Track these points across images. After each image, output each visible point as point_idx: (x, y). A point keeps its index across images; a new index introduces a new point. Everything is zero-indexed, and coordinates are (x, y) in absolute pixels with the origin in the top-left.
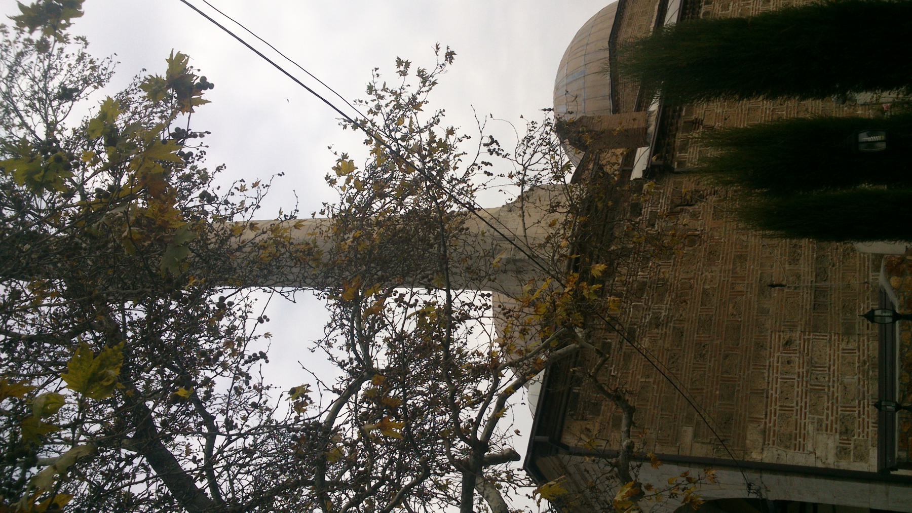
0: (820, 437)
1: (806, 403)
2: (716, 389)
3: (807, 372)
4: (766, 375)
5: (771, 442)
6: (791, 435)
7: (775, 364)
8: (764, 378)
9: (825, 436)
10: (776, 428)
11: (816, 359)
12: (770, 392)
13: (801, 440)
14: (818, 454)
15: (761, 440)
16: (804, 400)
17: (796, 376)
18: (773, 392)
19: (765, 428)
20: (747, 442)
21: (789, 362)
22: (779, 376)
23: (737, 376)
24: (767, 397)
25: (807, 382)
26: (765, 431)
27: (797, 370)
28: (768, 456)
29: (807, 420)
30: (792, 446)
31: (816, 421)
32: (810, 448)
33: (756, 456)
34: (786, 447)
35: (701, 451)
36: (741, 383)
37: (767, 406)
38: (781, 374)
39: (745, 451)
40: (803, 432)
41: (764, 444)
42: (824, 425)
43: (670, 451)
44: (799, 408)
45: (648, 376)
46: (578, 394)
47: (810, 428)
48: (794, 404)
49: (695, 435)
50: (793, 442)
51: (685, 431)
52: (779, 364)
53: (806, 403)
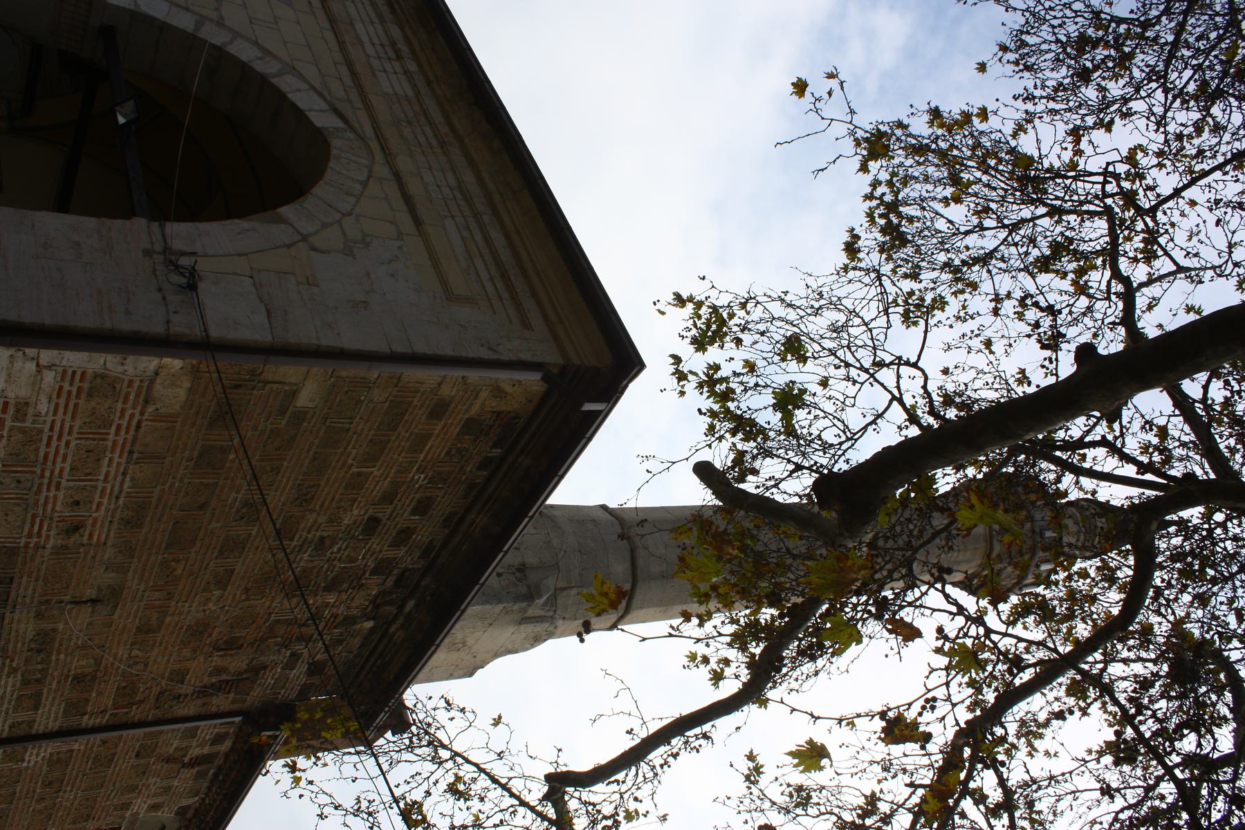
0: (24, 392)
1: (48, 445)
2: (233, 461)
3: (39, 491)
4: (127, 483)
5: (136, 384)
6: (90, 395)
7: (105, 501)
8: (133, 479)
9: (12, 395)
10: (119, 406)
11: (17, 509)
12: (123, 460)
13: (66, 387)
14: (32, 366)
15: (158, 387)
16: (52, 450)
17: (64, 483)
18: (116, 460)
19: (144, 407)
20: (187, 385)
21: (78, 503)
22: (100, 484)
23: (186, 480)
24: (131, 452)
25: (42, 476)
26: (146, 402)
27: (61, 495)
28: (148, 363)
29: (50, 418)
30: (88, 377)
31: (30, 418)
32: (49, 377)
33: (175, 364)
34: (103, 377)
35: (290, 372)
36: (181, 472)
37: (135, 439)
38: (95, 487)
39: (195, 372)
40: (62, 402)
41: (152, 382)
42: (11, 411)
43: (350, 371)
44: (65, 438)
45: (359, 474)
46: (495, 446)
47: (43, 407)
48: (73, 444)
49: (294, 394)
50: (86, 385)
51: (311, 400)
52: (97, 499)
53: (48, 445)
